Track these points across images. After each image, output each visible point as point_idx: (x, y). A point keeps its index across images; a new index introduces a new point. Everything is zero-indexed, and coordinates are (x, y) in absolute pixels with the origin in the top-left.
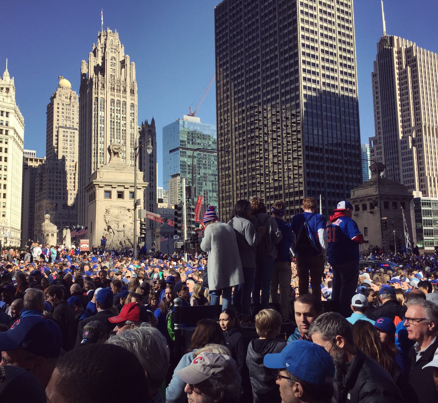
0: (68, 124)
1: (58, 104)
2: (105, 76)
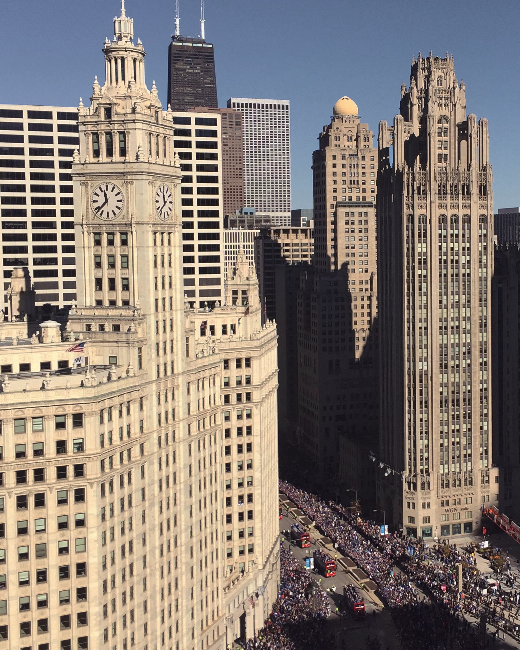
0: (355, 195)
1: (334, 157)
2: (428, 169)
